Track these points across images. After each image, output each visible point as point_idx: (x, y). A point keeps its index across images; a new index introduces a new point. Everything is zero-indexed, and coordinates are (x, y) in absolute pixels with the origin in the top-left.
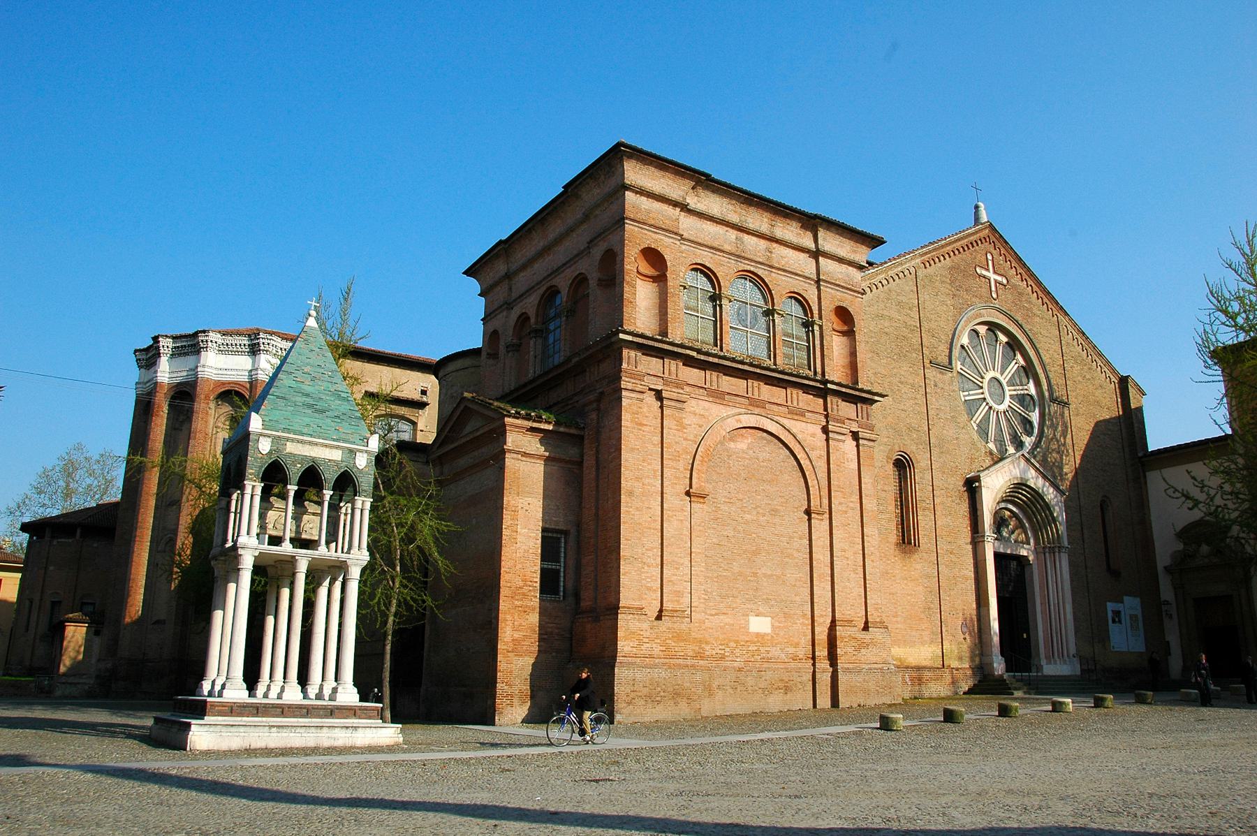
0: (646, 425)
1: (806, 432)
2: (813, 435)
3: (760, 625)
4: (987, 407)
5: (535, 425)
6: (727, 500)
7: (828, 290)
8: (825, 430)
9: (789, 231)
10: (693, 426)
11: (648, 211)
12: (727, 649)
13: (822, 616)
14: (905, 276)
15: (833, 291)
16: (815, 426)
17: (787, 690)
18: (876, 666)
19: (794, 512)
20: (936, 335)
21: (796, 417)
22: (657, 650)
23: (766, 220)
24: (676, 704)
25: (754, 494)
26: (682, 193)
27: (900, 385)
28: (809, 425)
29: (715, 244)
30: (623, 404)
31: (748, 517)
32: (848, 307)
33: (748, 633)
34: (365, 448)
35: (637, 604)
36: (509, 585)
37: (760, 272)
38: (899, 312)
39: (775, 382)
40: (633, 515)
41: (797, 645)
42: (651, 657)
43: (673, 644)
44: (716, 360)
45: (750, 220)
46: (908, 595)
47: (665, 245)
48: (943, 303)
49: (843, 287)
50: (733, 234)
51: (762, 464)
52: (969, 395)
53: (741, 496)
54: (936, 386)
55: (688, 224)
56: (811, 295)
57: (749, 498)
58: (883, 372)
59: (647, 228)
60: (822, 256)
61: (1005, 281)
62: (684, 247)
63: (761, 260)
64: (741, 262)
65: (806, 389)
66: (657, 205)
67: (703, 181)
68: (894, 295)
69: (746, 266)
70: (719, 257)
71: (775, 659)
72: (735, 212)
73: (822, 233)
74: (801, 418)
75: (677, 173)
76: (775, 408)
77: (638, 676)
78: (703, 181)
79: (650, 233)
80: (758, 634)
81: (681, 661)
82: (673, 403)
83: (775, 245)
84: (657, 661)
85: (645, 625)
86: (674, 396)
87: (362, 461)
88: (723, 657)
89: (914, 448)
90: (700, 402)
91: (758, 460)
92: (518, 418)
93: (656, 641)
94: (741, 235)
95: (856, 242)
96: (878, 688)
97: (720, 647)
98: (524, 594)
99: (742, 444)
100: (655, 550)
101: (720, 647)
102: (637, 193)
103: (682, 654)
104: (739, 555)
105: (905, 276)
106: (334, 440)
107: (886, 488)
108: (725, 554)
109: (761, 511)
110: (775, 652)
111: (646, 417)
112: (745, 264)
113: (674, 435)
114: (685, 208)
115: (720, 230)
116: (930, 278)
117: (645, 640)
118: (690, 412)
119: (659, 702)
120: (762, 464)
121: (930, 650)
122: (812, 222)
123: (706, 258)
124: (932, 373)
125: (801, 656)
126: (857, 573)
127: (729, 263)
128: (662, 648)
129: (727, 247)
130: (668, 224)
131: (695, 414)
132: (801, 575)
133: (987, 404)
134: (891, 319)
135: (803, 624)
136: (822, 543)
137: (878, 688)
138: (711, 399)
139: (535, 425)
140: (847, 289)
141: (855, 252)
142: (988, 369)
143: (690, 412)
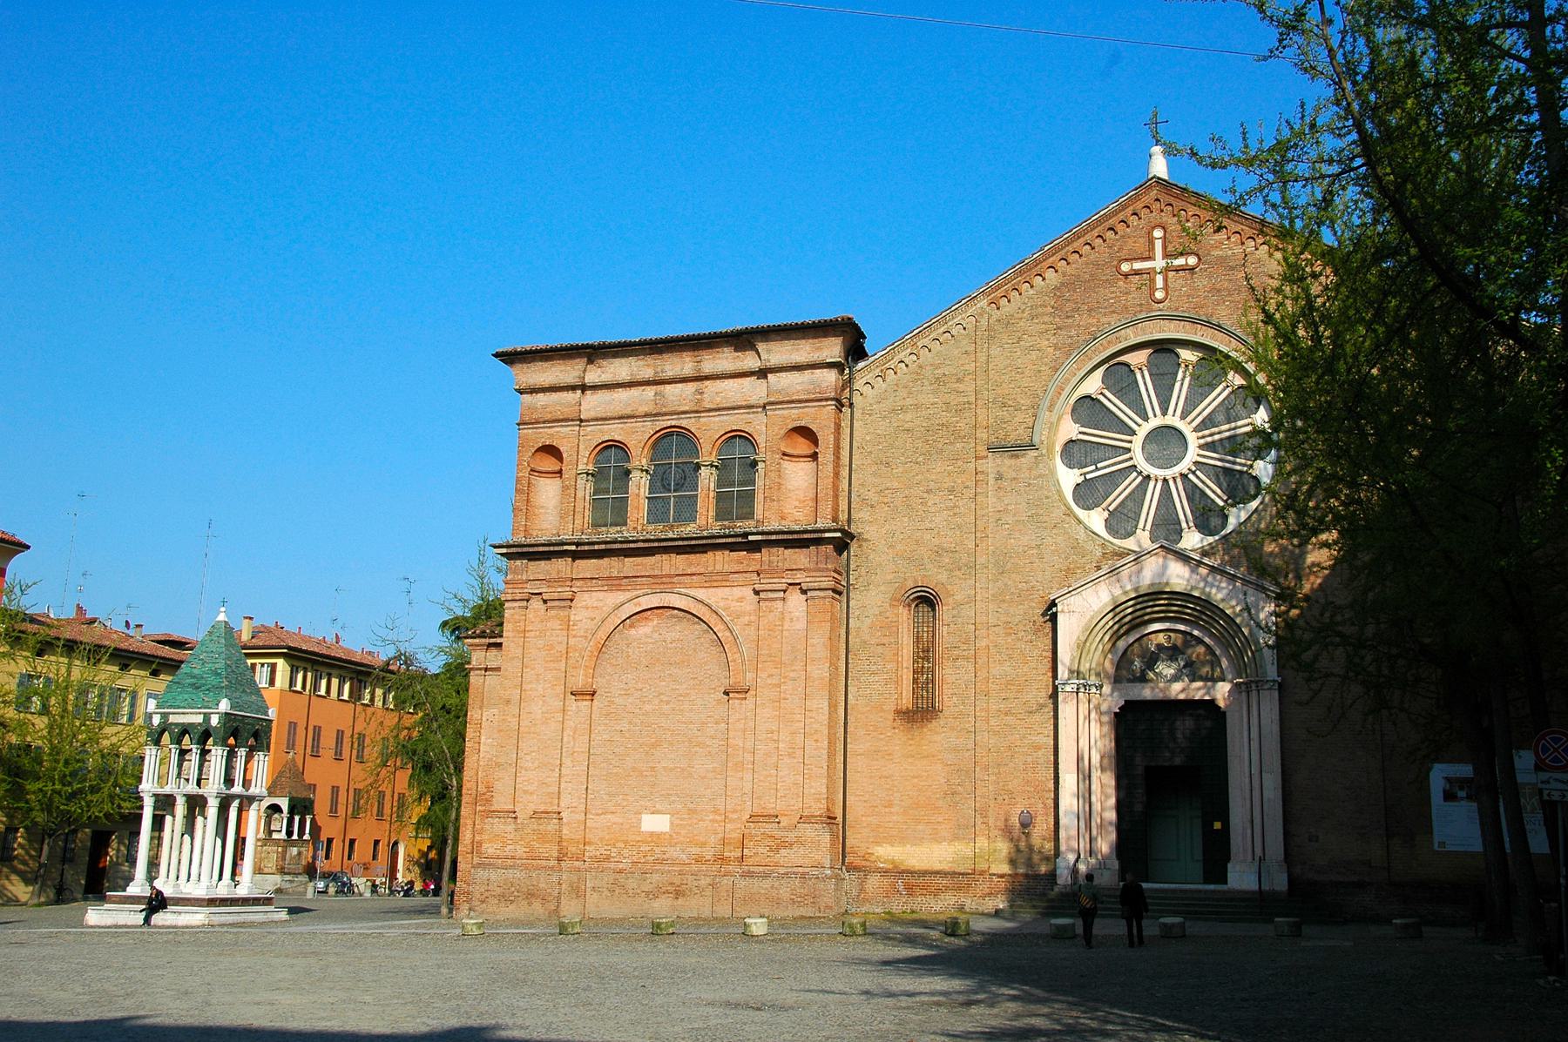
0: (532, 631)
1: (730, 598)
2: (741, 600)
3: (655, 823)
4: (1140, 478)
5: (492, 641)
6: (623, 693)
7: (777, 412)
8: (757, 593)
9: (725, 360)
10: (584, 620)
11: (544, 407)
12: (614, 850)
13: (735, 811)
14: (953, 336)
15: (785, 412)
16: (744, 589)
17: (678, 894)
18: (800, 870)
19: (710, 694)
20: (1010, 403)
21: (715, 584)
22: (521, 851)
23: (688, 359)
24: (530, 904)
25: (657, 681)
26: (577, 374)
27: (925, 495)
28: (735, 589)
29: (628, 411)
30: (507, 614)
31: (648, 707)
32: (808, 425)
33: (640, 833)
34: (216, 711)
35: (511, 807)
36: (470, 792)
37: (684, 423)
38: (935, 392)
39: (689, 550)
40: (510, 722)
41: (703, 845)
42: (513, 858)
43: (538, 845)
44: (603, 547)
45: (667, 367)
46: (914, 777)
47: (562, 436)
48: (1031, 348)
49: (800, 401)
50: (650, 392)
51: (670, 645)
52: (1097, 469)
53: (640, 686)
54: (999, 477)
55: (593, 404)
56: (757, 425)
57: (650, 686)
58: (896, 485)
59: (542, 425)
60: (771, 373)
61: (1192, 261)
62: (589, 429)
63: (687, 408)
64: (658, 420)
65: (732, 547)
66: (555, 396)
67: (594, 353)
68: (928, 372)
69: (662, 423)
70: (631, 424)
71: (672, 860)
72: (648, 365)
73: (761, 347)
74: (724, 583)
75: (563, 357)
76: (687, 579)
77: (493, 877)
78: (594, 353)
79: (546, 430)
80: (652, 834)
81: (544, 863)
82: (557, 603)
83: (707, 383)
84: (518, 862)
85: (510, 828)
86: (556, 596)
87: (215, 721)
88: (608, 858)
89: (943, 577)
90: (594, 594)
91: (665, 641)
92: (485, 637)
93: (520, 843)
94: (660, 388)
95: (815, 337)
96: (792, 897)
97: (606, 847)
98: (487, 800)
99: (644, 630)
100: (534, 754)
101: (606, 847)
102: (531, 393)
103: (547, 855)
104: (635, 750)
105: (953, 336)
106: (199, 708)
107: (885, 640)
108: (616, 750)
109: (665, 699)
110: (674, 853)
111: (532, 622)
112: (663, 420)
113: (557, 636)
114: (584, 388)
115: (635, 392)
116: (1007, 323)
117: (510, 842)
118: (581, 607)
119: (512, 902)
120: (670, 645)
121: (951, 849)
122: (743, 339)
123: (614, 432)
124: (991, 464)
125: (708, 857)
126: (794, 757)
127: (643, 426)
128: (525, 850)
129: (643, 409)
130: (568, 412)
131: (587, 608)
132: (715, 765)
133: (1140, 473)
134: (917, 407)
135: (713, 821)
136: (742, 726)
137: (792, 897)
138: (606, 588)
139: (492, 641)
140: (807, 401)
141: (819, 349)
142: (1150, 414)
143: (581, 607)
